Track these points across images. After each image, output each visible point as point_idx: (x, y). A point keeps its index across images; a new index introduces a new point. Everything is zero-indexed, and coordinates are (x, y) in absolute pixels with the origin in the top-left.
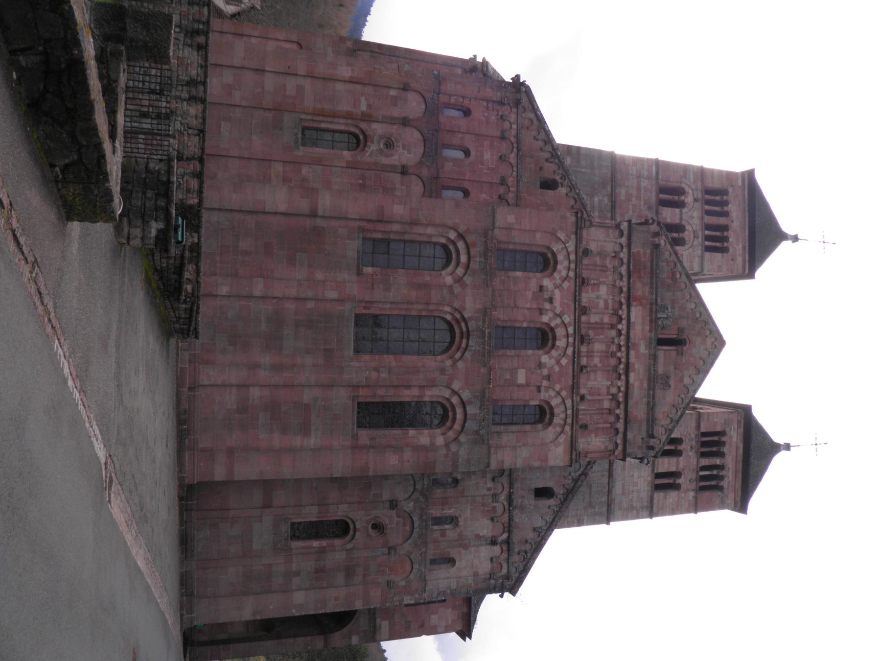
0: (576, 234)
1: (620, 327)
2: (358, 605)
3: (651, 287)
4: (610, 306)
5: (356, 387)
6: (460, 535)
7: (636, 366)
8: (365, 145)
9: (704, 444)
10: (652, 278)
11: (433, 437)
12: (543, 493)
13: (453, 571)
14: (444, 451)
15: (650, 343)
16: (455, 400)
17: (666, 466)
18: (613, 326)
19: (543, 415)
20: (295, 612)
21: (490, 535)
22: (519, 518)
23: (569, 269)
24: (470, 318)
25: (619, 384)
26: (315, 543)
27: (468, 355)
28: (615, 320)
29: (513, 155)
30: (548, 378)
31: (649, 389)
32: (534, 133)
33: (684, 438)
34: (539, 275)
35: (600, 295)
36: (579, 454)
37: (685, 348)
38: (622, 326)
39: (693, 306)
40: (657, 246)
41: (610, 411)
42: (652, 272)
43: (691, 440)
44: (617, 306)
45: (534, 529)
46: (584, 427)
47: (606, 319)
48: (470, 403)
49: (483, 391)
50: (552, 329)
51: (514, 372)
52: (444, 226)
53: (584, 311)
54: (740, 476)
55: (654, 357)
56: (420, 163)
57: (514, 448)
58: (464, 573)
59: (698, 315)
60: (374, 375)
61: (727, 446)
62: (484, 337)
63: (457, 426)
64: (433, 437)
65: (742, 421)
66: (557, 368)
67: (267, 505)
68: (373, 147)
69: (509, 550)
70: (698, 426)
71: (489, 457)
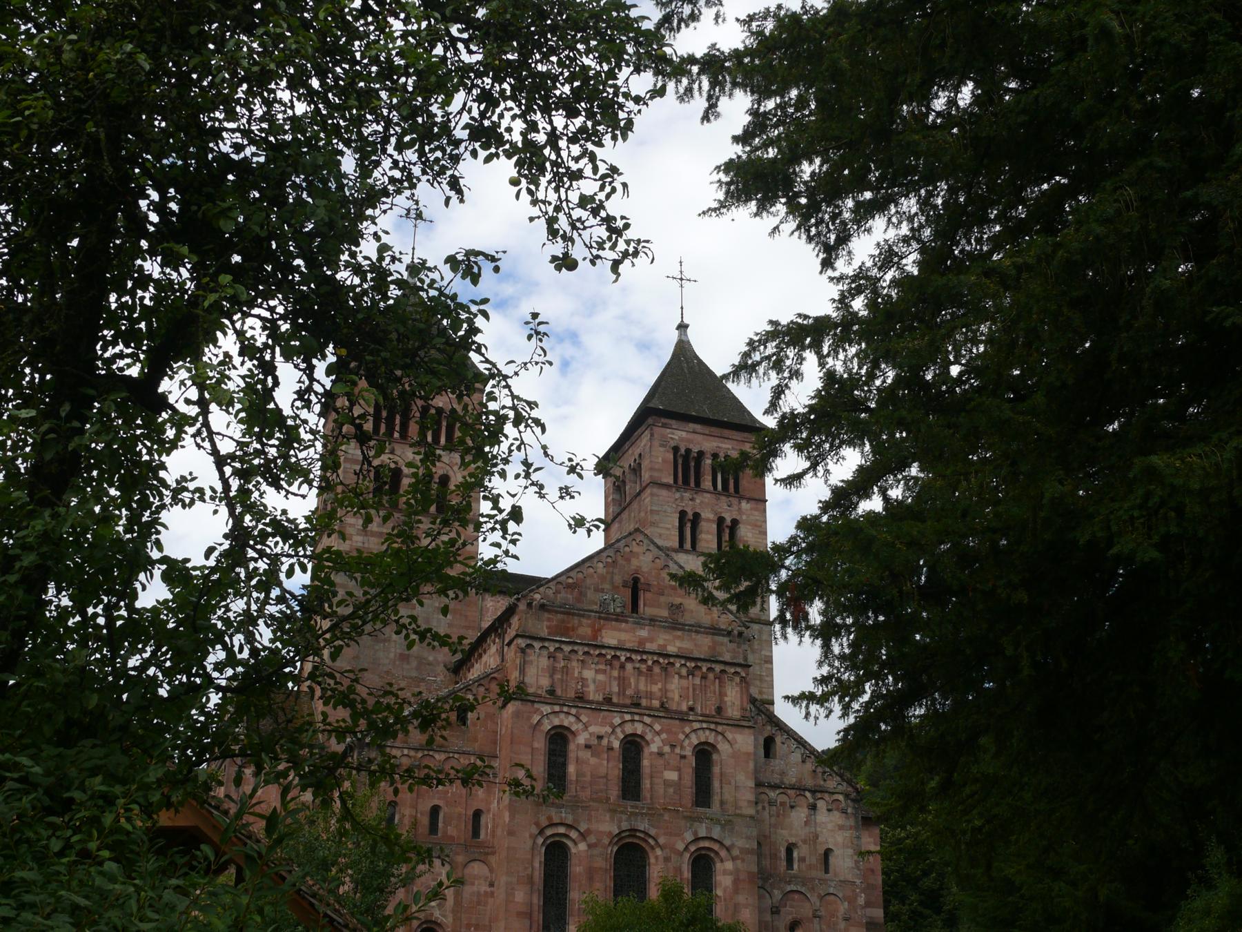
0: (533, 702)
1: (623, 659)
3: (583, 616)
4: (602, 667)
6: (805, 842)
7: (661, 642)
8: (435, 923)
10: (574, 614)
11: (725, 872)
12: (769, 746)
14: (739, 862)
15: (638, 623)
16: (693, 848)
17: (710, 537)
18: (622, 667)
19: (704, 754)
21: (806, 810)
22: (791, 779)
23: (568, 713)
24: (619, 827)
25: (678, 665)
27: (653, 832)
29: (437, 756)
31: (683, 630)
33: (680, 509)
34: (572, 747)
35: (593, 678)
36: (744, 718)
37: (642, 580)
39: (600, 565)
40: (542, 607)
41: (704, 677)
42: (568, 614)
43: (682, 498)
44: (602, 660)
45: (803, 762)
46: (719, 710)
47: (615, 673)
48: (695, 833)
49: (685, 817)
50: (626, 737)
52: (533, 849)
53: (608, 700)
54: (727, 432)
55: (653, 621)
57: (737, 788)
58: (840, 839)
59: (609, 560)
61: (691, 446)
62: (636, 814)
63: (716, 847)
64: (725, 872)
65: (663, 420)
66: (664, 736)
68: (437, 914)
69: (822, 792)
70: (666, 486)
71: (745, 816)
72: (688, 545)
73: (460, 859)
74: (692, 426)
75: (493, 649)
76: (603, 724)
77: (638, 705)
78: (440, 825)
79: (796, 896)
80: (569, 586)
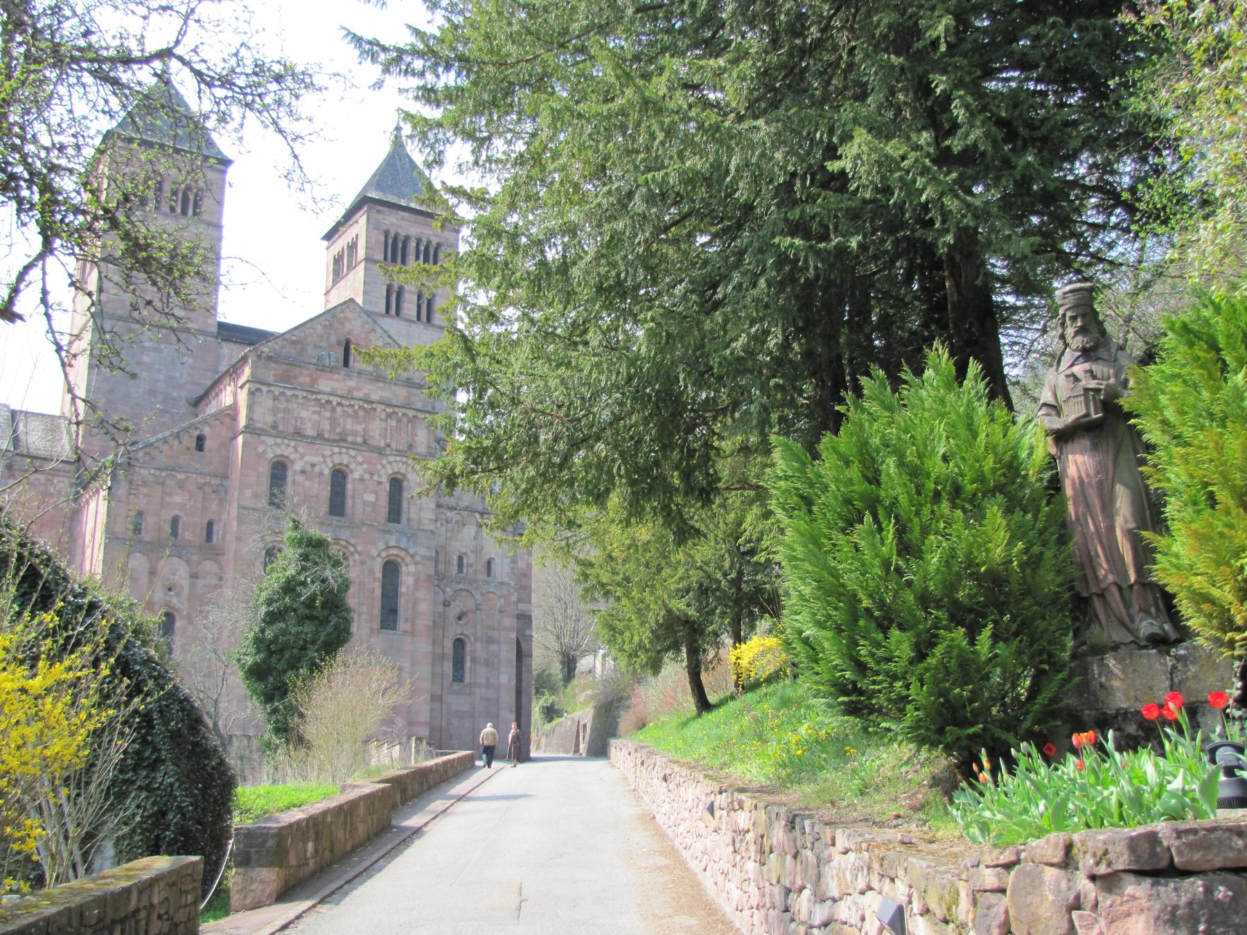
2: (514, 635)
5: (372, 631)
6: (472, 552)
7: (366, 391)
9: (394, 260)
13: (498, 560)
14: (420, 566)
16: (384, 554)
18: (333, 410)
20: (514, 682)
26: (468, 664)
27: (353, 541)
28: (328, 407)
30: (372, 474)
32: (156, 453)
34: (289, 473)
35: (309, 418)
38: (335, 400)
39: (319, 327)
41: (399, 421)
42: (291, 365)
47: (328, 414)
51: (365, 503)
53: (320, 436)
55: (360, 373)
56: (187, 561)
57: (421, 509)
60: (364, 617)
63: (402, 554)
64: (408, 574)
66: (365, 466)
67: (440, 699)
68: (175, 601)
72: (393, 311)
73: (195, 558)
74: (401, 213)
75: (229, 389)
76: (316, 455)
77: (345, 440)
78: (180, 531)
79: (464, 593)
80: (293, 342)
